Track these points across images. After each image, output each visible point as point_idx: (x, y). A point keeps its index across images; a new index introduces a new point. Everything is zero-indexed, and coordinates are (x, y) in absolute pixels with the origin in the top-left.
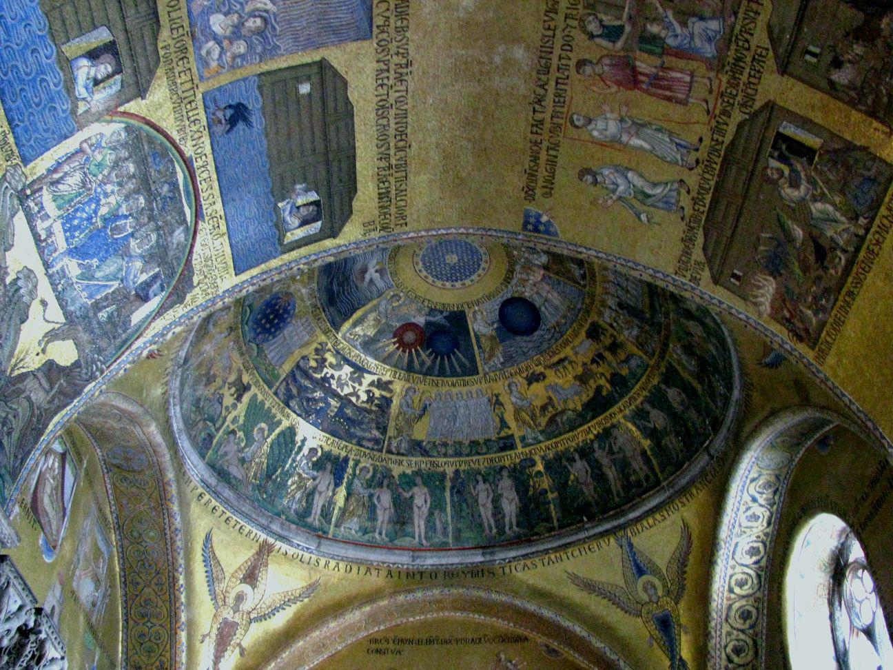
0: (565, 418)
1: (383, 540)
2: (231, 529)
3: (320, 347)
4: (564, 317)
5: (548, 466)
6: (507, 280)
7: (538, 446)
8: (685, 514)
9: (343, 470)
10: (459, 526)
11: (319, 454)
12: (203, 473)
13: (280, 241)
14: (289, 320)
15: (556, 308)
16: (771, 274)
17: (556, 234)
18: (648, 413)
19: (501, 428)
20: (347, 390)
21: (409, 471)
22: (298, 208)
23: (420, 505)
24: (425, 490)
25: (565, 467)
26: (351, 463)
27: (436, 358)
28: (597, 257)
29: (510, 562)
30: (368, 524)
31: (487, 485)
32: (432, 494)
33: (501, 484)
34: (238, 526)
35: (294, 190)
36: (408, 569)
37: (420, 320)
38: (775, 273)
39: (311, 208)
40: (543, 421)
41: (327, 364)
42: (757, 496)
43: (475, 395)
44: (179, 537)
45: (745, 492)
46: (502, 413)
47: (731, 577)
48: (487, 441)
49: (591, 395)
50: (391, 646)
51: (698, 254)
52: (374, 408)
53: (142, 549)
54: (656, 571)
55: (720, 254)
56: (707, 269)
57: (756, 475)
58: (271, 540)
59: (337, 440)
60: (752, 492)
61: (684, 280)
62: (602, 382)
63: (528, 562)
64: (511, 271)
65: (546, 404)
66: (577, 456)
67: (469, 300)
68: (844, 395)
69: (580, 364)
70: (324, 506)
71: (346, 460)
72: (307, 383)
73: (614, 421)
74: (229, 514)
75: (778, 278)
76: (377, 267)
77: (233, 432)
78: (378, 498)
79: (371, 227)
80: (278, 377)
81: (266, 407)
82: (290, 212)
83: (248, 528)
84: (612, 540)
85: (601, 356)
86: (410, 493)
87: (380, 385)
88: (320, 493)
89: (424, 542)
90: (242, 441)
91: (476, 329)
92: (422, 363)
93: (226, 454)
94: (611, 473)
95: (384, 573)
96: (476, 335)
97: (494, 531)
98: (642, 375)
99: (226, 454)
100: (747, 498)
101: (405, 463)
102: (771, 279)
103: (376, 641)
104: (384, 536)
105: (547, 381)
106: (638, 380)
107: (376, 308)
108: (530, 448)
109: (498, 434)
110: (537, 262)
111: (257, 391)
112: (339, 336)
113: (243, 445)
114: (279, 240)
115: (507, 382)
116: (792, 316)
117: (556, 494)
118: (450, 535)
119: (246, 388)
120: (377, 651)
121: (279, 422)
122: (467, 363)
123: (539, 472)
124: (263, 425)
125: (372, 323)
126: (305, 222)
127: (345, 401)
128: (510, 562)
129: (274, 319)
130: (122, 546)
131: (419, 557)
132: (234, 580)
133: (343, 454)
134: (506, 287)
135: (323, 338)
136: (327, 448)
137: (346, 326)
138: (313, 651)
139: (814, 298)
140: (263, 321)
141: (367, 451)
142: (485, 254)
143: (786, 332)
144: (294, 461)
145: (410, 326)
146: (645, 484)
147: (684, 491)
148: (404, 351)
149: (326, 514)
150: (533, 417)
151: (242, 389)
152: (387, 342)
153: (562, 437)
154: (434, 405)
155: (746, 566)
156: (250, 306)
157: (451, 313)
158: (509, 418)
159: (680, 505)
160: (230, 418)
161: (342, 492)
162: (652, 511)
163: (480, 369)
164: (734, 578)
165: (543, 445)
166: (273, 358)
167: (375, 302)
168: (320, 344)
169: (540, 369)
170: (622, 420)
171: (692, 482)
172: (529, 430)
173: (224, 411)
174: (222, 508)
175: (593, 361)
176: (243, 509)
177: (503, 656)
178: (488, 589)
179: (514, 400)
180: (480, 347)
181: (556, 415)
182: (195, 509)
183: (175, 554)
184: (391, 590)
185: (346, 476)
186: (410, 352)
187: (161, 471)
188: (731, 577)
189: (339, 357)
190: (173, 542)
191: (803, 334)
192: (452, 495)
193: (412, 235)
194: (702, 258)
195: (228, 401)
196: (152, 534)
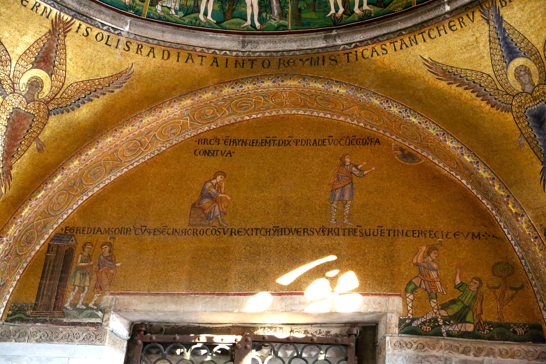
1: (208, 21)
29: (354, 47)
36: (237, 56)
50: (221, 147)
58: (66, 17)
63: (378, 47)
84: (477, 14)
89: (257, 24)
95: (208, 61)
97: (341, 10)
103: (205, 141)
104: (209, 17)
118: (290, 16)
120: (206, 153)
128: (356, 46)
131: (250, 42)
132: (22, 63)
138: (130, 150)
177: (348, 160)
178: (328, 80)
184: (215, 80)
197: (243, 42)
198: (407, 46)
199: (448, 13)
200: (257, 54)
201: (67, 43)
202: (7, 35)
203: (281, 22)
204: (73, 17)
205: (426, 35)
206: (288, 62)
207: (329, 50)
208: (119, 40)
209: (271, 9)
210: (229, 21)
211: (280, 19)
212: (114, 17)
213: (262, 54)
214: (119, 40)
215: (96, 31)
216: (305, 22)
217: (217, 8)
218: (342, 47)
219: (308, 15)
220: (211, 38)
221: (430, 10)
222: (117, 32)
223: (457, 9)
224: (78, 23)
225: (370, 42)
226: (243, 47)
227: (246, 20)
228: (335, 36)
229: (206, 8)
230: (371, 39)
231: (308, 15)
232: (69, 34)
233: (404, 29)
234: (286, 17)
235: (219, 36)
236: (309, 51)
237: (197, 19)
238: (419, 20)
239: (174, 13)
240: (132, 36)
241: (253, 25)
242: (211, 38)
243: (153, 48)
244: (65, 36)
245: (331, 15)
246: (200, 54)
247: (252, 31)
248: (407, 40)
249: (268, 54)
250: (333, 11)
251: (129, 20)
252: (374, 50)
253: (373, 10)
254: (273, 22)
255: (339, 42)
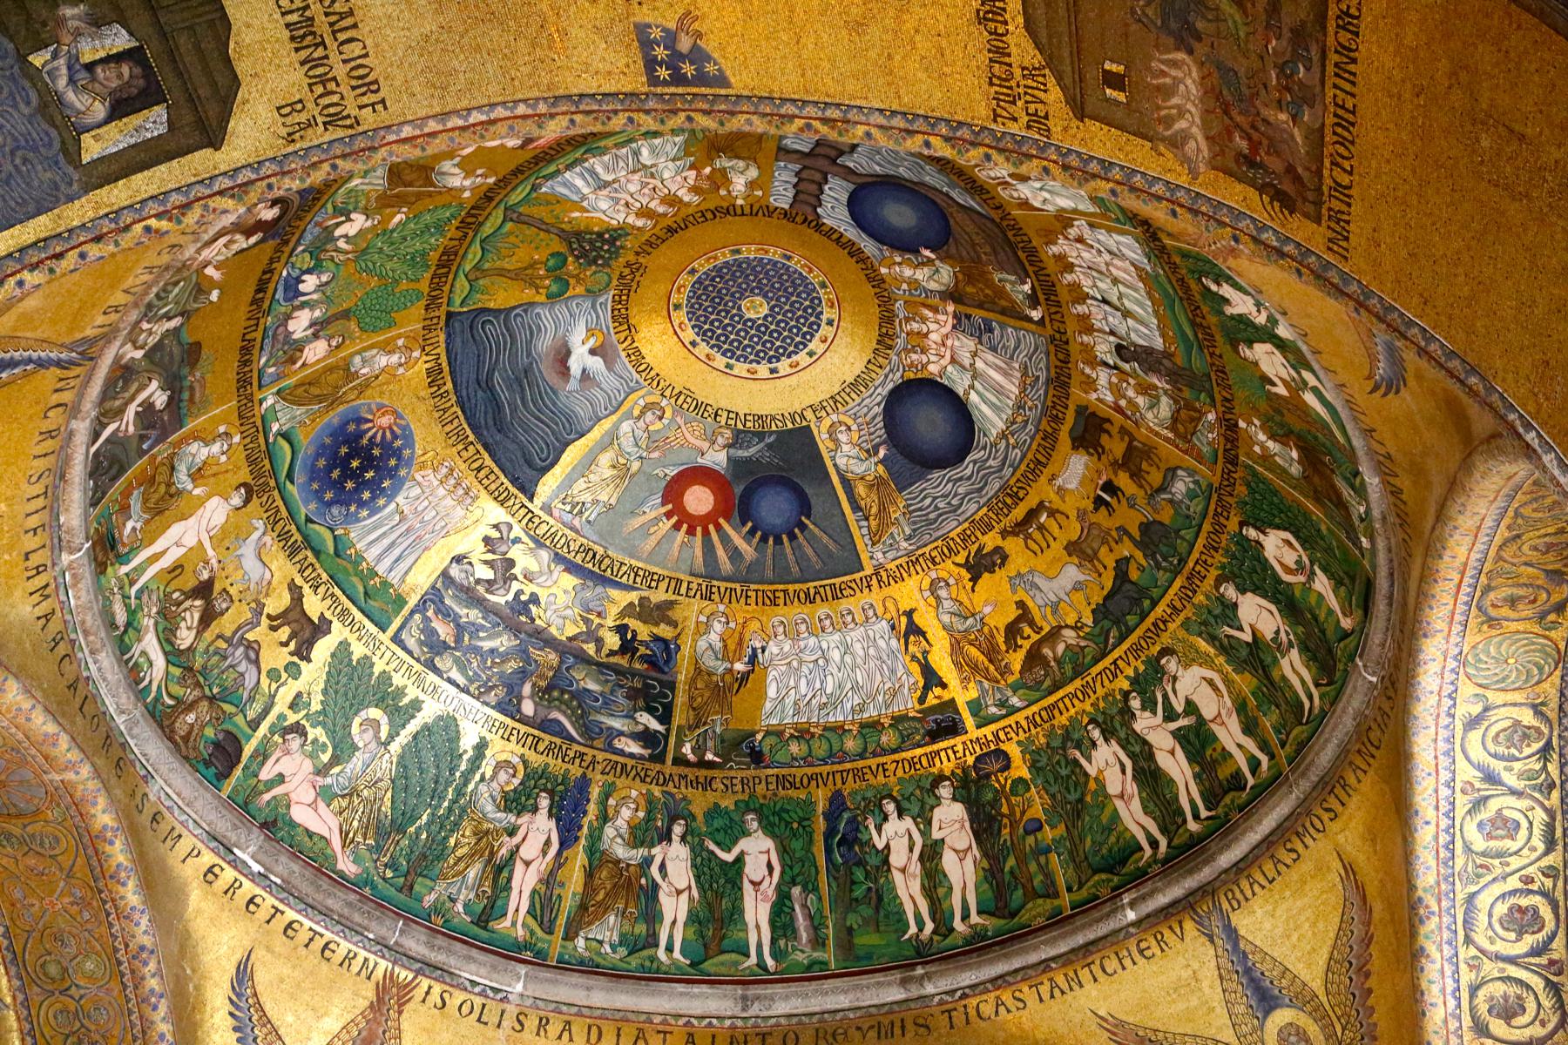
0: (1061, 648)
1: (674, 962)
2: (303, 951)
3: (495, 534)
4: (1020, 406)
5: (1034, 767)
6: (885, 341)
7: (1011, 720)
8: (1341, 838)
9: (579, 808)
10: (852, 920)
11: (521, 774)
12: (213, 816)
13: (71, 151)
14: (402, 473)
15: (999, 391)
16: (1182, 44)
17: (722, 81)
18: (1235, 605)
19: (927, 688)
20: (571, 630)
21: (727, 803)
22: (90, 67)
23: (757, 879)
24: (768, 844)
25: (1076, 762)
26: (595, 792)
27: (764, 539)
28: (824, 121)
29: (962, 998)
30: (641, 929)
31: (908, 822)
32: (783, 850)
33: (938, 814)
34: (319, 943)
35: (61, 22)
36: (733, 1027)
37: (717, 458)
38: (1186, 38)
39: (125, 70)
40: (1016, 660)
41: (517, 571)
42: (1497, 766)
43: (859, 618)
44: (152, 966)
45: (1459, 756)
46: (925, 653)
47: (1474, 990)
48: (898, 720)
49: (1109, 584)
51: (1023, 51)
52: (637, 666)
53: (72, 1006)
54: (1303, 999)
55: (1063, 28)
56: (1051, 82)
57: (1476, 709)
58: (404, 975)
59: (558, 741)
60: (1477, 753)
61: (1014, 128)
62: (1126, 549)
63: (1006, 996)
64: (887, 318)
65: (1018, 620)
66: (1096, 734)
67: (815, 400)
68: (1411, 323)
69: (1073, 514)
70: (534, 891)
71: (584, 784)
72: (473, 615)
73: (1165, 640)
74: (291, 915)
75: (1196, 45)
76: (591, 343)
77: (298, 729)
78: (662, 867)
79: (303, 117)
80: (400, 601)
81: (377, 670)
82: (72, 81)
83: (344, 946)
84: (1189, 925)
85: (1109, 487)
86: (736, 851)
87: (647, 612)
88: (527, 864)
89: (770, 963)
90: (324, 747)
91: (841, 462)
92: (735, 555)
93: (281, 778)
94: (1176, 766)
96: (846, 482)
97: (929, 926)
98: (1204, 515)
99: (281, 778)
100: (1466, 773)
101: (718, 785)
102: (1181, 56)
104: (677, 954)
105: (1012, 568)
106: (1200, 527)
107: (612, 438)
108: (993, 727)
109: (922, 700)
110: (933, 286)
111: (346, 633)
112: (535, 506)
113: (325, 758)
114: (64, 150)
115: (926, 583)
116: (1254, 146)
117: (1061, 830)
118: (831, 942)
119: (321, 628)
121: (416, 705)
122: (832, 546)
123: (1020, 781)
124: (374, 713)
125: (609, 473)
126: (120, 108)
127: (569, 651)
128: (962, 998)
129: (363, 468)
130: (26, 1004)
131: (758, 998)
133: (576, 771)
134: (887, 357)
135: (497, 513)
136: (536, 760)
137: (548, 485)
139: (1281, 69)
140: (335, 474)
141: (630, 762)
142: (823, 286)
143: (1253, 194)
144: (460, 793)
145: (697, 474)
146: (1251, 781)
147: (1331, 785)
148: (691, 532)
149: (543, 906)
150: (991, 653)
151: (306, 632)
152: (653, 514)
153: (1060, 693)
154: (773, 648)
155: (1512, 960)
156: (286, 436)
157: (781, 434)
158: (942, 662)
159: (1326, 816)
160: (285, 695)
161: (579, 858)
162: (1268, 844)
163: (864, 557)
164: (1481, 993)
165: (1020, 717)
166: (379, 559)
167: (606, 424)
168: (496, 527)
169: (990, 541)
170: (1182, 634)
171: (1343, 753)
172: (986, 684)
173: (265, 681)
174: (271, 901)
175: (1099, 502)
176: (330, 902)
179: (946, 618)
180: (856, 507)
181: (1040, 643)
182: (199, 904)
183: (148, 1011)
185: (585, 821)
186: (706, 533)
187: (78, 808)
188: (1474, 990)
189: (545, 555)
190: (138, 981)
191: (1287, 187)
192: (828, 851)
193: (407, 131)
194: (1033, 57)
195: (275, 656)
196: (89, 966)
197: (744, 998)
198: (1063, 993)
199: (1133, 924)
200: (773, 1021)
201: (405, 1025)
202: (290, 1019)
203: (815, 954)
204: (418, 973)
205: (1096, 968)
206: (834, 1035)
207: (913, 1005)
208: (503, 1012)
209: (795, 931)
210: (715, 960)
211: (814, 949)
212: (494, 968)
213: (783, 1021)
214: (503, 1012)
215: (459, 997)
216: (861, 953)
217: (691, 935)
218: (937, 999)
219: (866, 939)
220: (682, 994)
221: (1098, 921)
222: (500, 996)
223: (1148, 916)
224: (425, 983)
225: (989, 986)
226: (744, 1010)
227: (748, 956)
228: (922, 977)
229: (671, 937)
230: (993, 980)
231: (866, 939)
232: (407, 1007)
233: (1053, 959)
234: (824, 945)
235: (696, 989)
236: (873, 1010)
237: (653, 959)
238: (1080, 939)
239: (609, 950)
240: (529, 1002)
241: (761, 965)
242: (682, 994)
243: (568, 1023)
244: (400, 1013)
245: (910, 939)
246: (660, 1028)
247: (761, 978)
248: (1060, 980)
249: (794, 1020)
250: (913, 930)
251: (522, 969)
252: (999, 1003)
253: (990, 923)
254: (800, 957)
255: (930, 989)
